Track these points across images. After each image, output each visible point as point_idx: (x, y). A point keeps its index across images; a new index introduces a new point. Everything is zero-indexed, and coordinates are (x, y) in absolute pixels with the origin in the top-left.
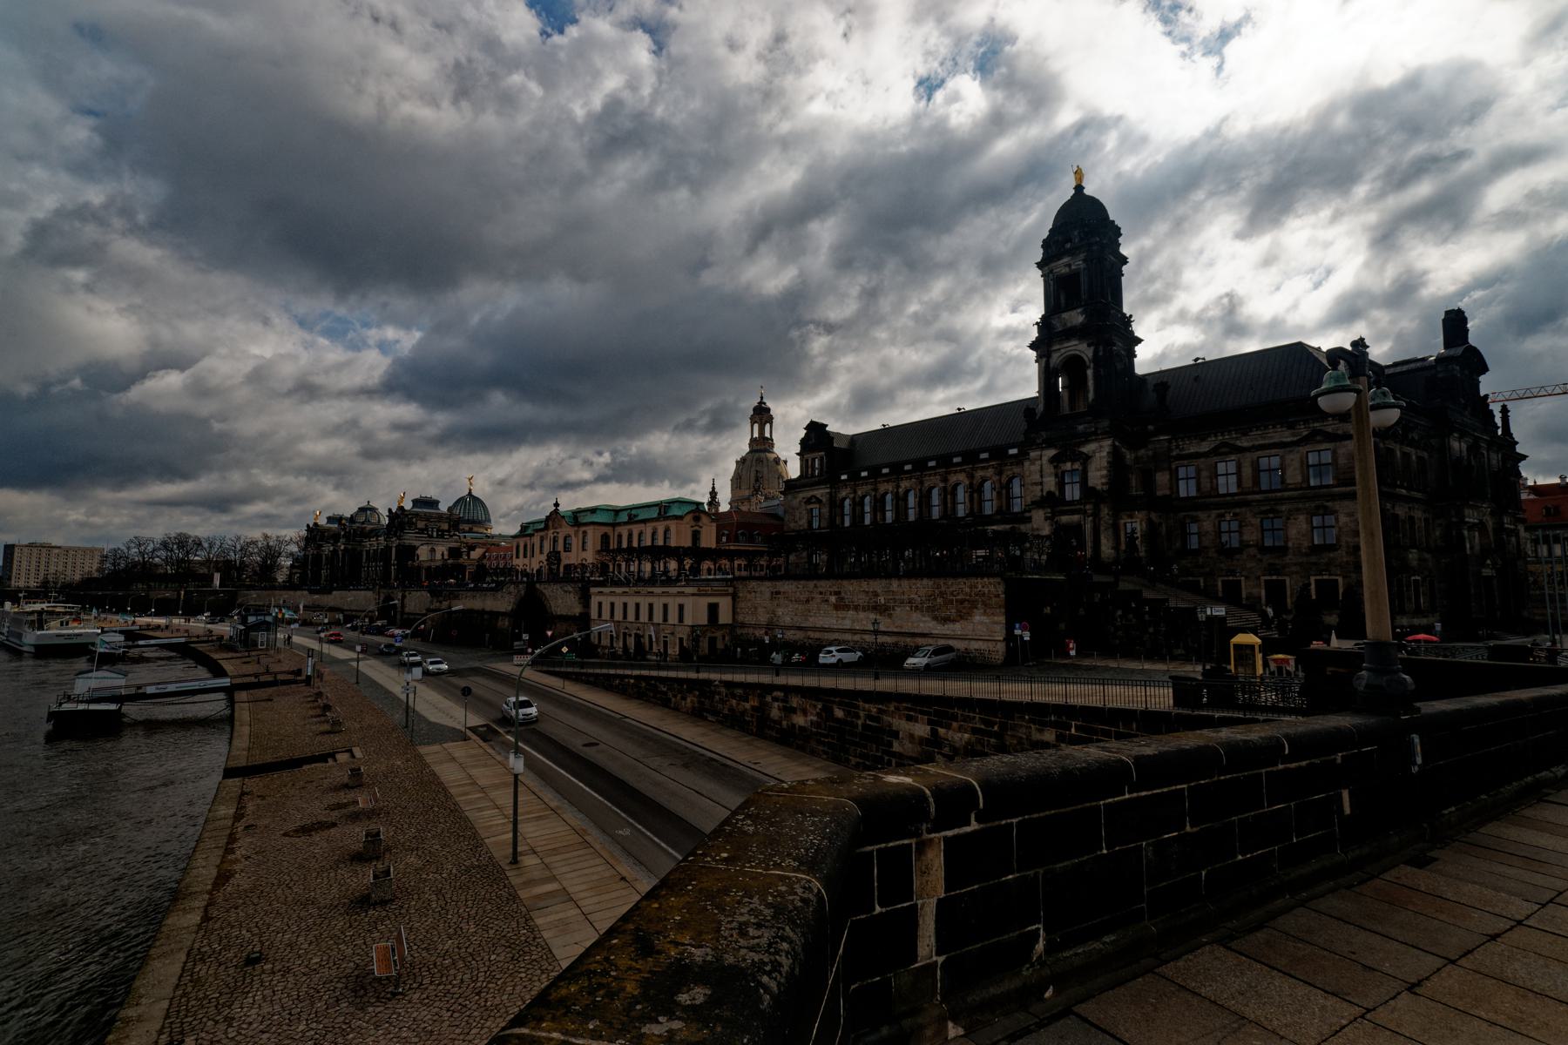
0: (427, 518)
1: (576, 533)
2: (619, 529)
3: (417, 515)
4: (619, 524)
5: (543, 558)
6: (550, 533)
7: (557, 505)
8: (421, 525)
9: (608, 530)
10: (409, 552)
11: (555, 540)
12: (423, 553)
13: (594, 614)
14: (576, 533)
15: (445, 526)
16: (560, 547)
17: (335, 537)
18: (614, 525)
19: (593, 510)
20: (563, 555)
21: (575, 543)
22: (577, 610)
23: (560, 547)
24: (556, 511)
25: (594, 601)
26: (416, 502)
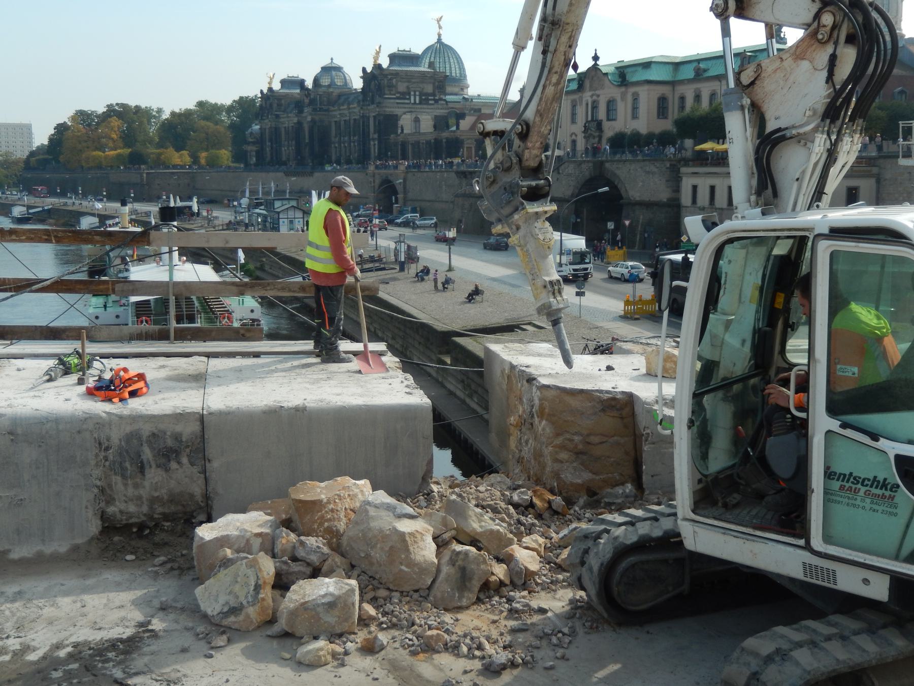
0: (409, 76)
1: (623, 97)
2: (680, 90)
3: (396, 74)
4: (682, 82)
5: (579, 128)
6: (587, 96)
7: (596, 58)
8: (402, 87)
9: (665, 90)
10: (389, 123)
11: (595, 106)
12: (406, 122)
13: (686, 198)
14: (623, 97)
15: (429, 89)
16: (602, 114)
17: (299, 106)
18: (673, 84)
19: (646, 65)
20: (606, 125)
21: (623, 109)
22: (664, 195)
23: (602, 114)
24: (596, 64)
25: (687, 184)
26: (393, 57)
